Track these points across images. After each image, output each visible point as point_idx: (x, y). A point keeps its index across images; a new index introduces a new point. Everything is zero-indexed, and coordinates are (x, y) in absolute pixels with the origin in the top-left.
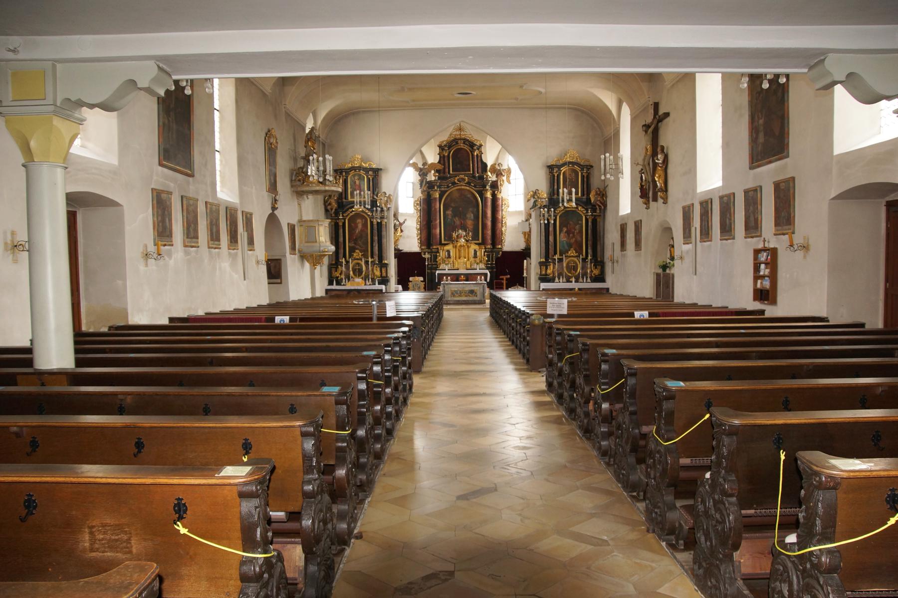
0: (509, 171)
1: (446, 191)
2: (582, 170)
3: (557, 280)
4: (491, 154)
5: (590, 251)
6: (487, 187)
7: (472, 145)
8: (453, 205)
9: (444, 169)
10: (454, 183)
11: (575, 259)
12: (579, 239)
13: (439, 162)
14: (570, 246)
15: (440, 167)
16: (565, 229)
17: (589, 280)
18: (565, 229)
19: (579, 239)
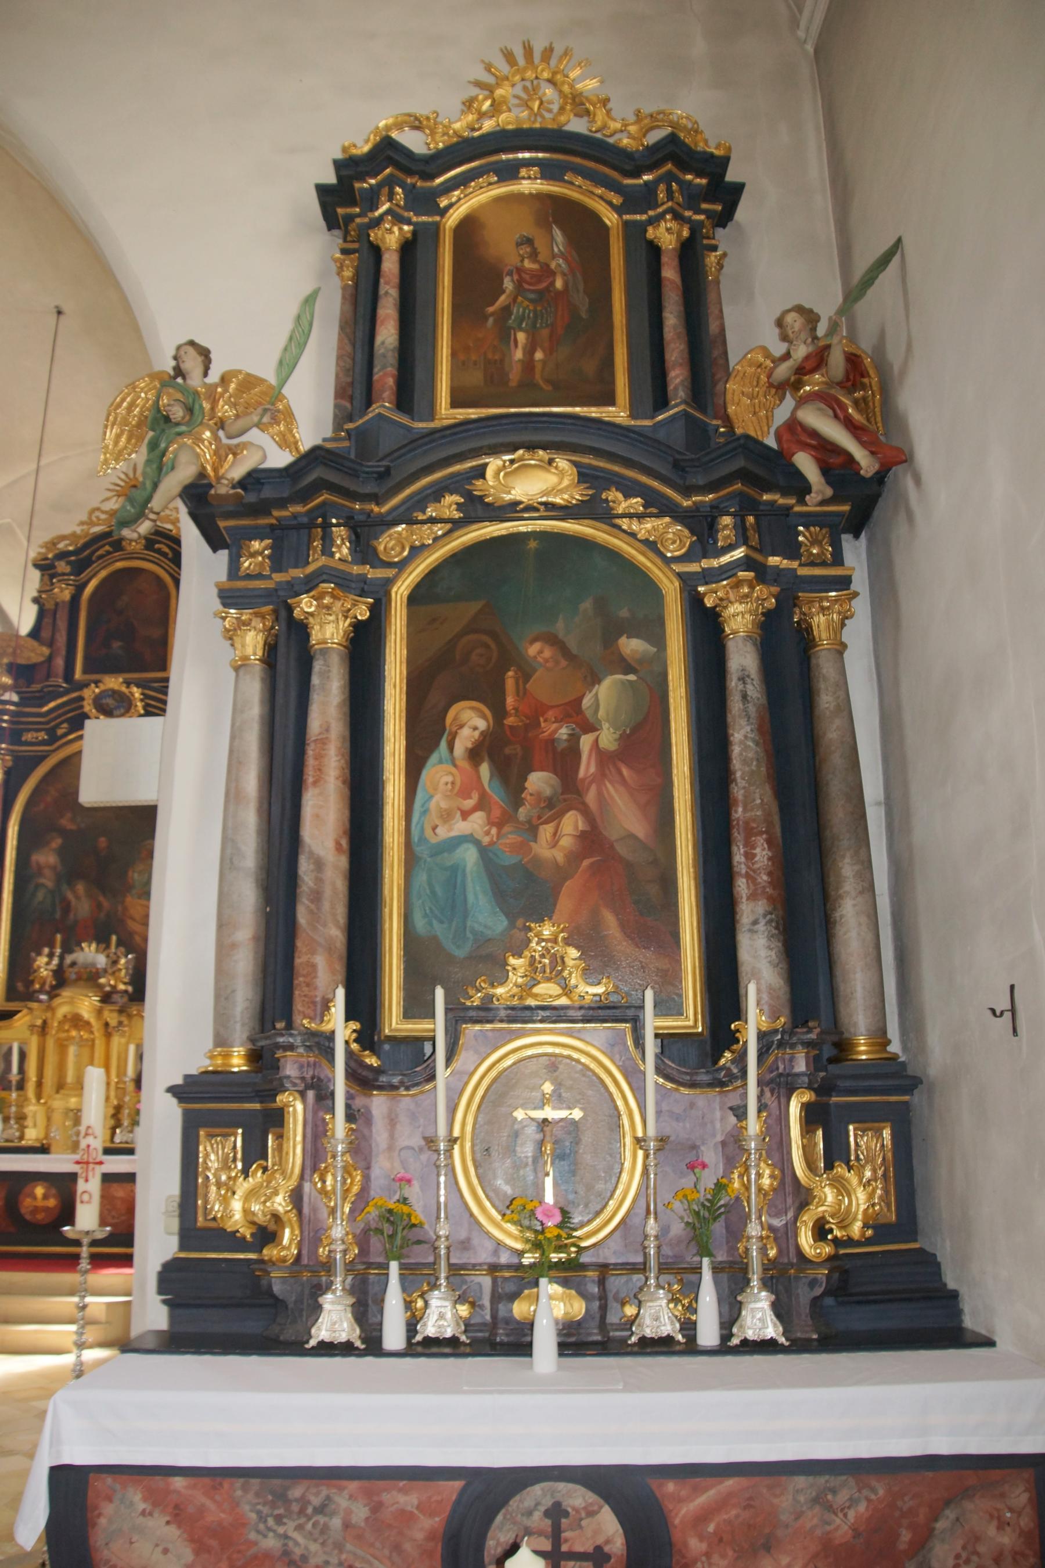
1: (41, 758)
2: (638, 200)
3: (334, 1320)
5: (759, 956)
8: (66, 822)
9: (50, 659)
11: (589, 1047)
12: (627, 818)
14: (526, 894)
15: (37, 653)
16: (470, 722)
17: (760, 1318)
18: (470, 722)
19: (627, 818)
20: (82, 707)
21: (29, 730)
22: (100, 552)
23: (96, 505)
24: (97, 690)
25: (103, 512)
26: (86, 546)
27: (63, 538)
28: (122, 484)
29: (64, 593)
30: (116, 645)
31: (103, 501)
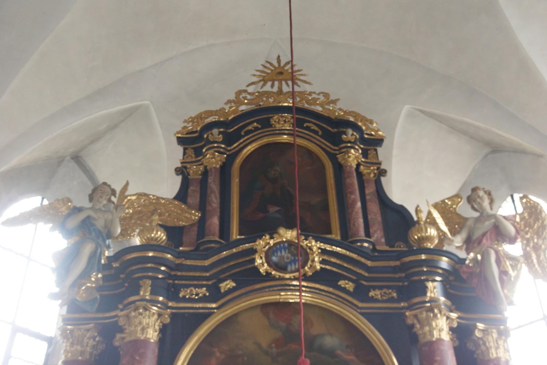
0: (538, 204)
4: (418, 177)
6: (434, 289)
7: (335, 128)
9: (202, 222)
10: (249, 277)
13: (182, 196)
20: (254, 260)
21: (188, 286)
22: (250, 128)
23: (244, 88)
24: (272, 242)
25: (249, 94)
26: (236, 120)
27: (210, 113)
28: (269, 72)
29: (213, 159)
30: (273, 209)
31: (248, 86)
